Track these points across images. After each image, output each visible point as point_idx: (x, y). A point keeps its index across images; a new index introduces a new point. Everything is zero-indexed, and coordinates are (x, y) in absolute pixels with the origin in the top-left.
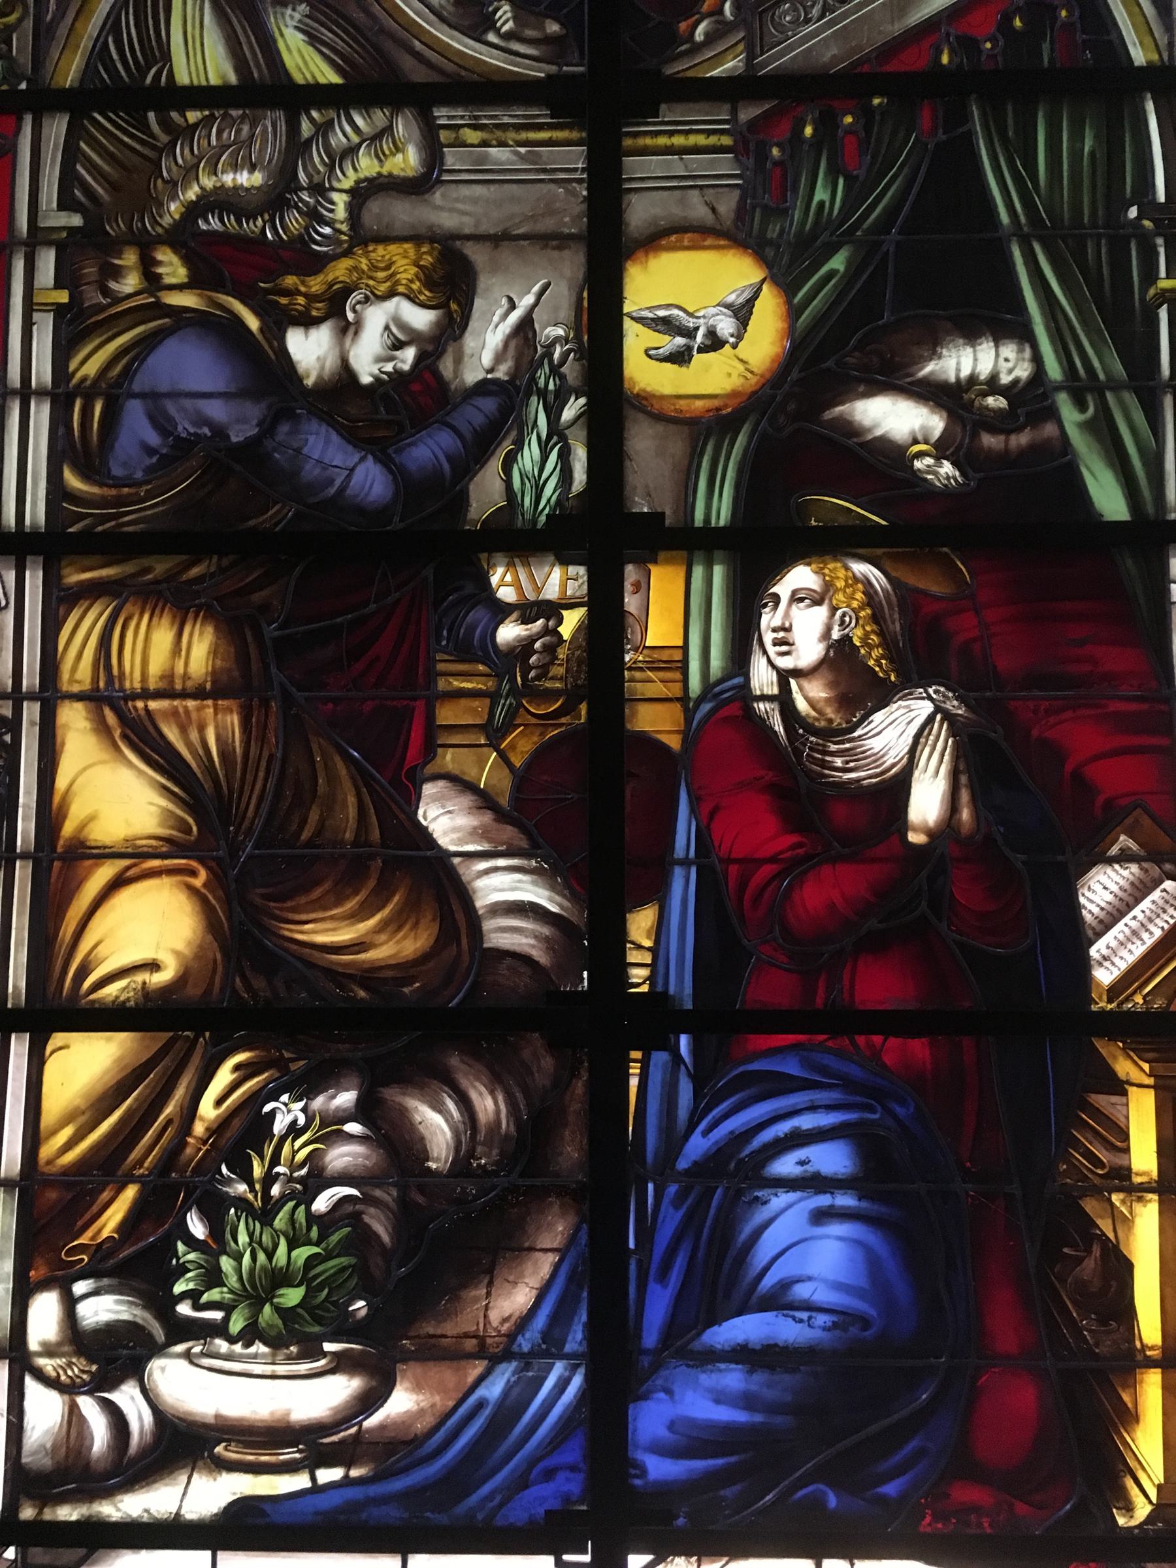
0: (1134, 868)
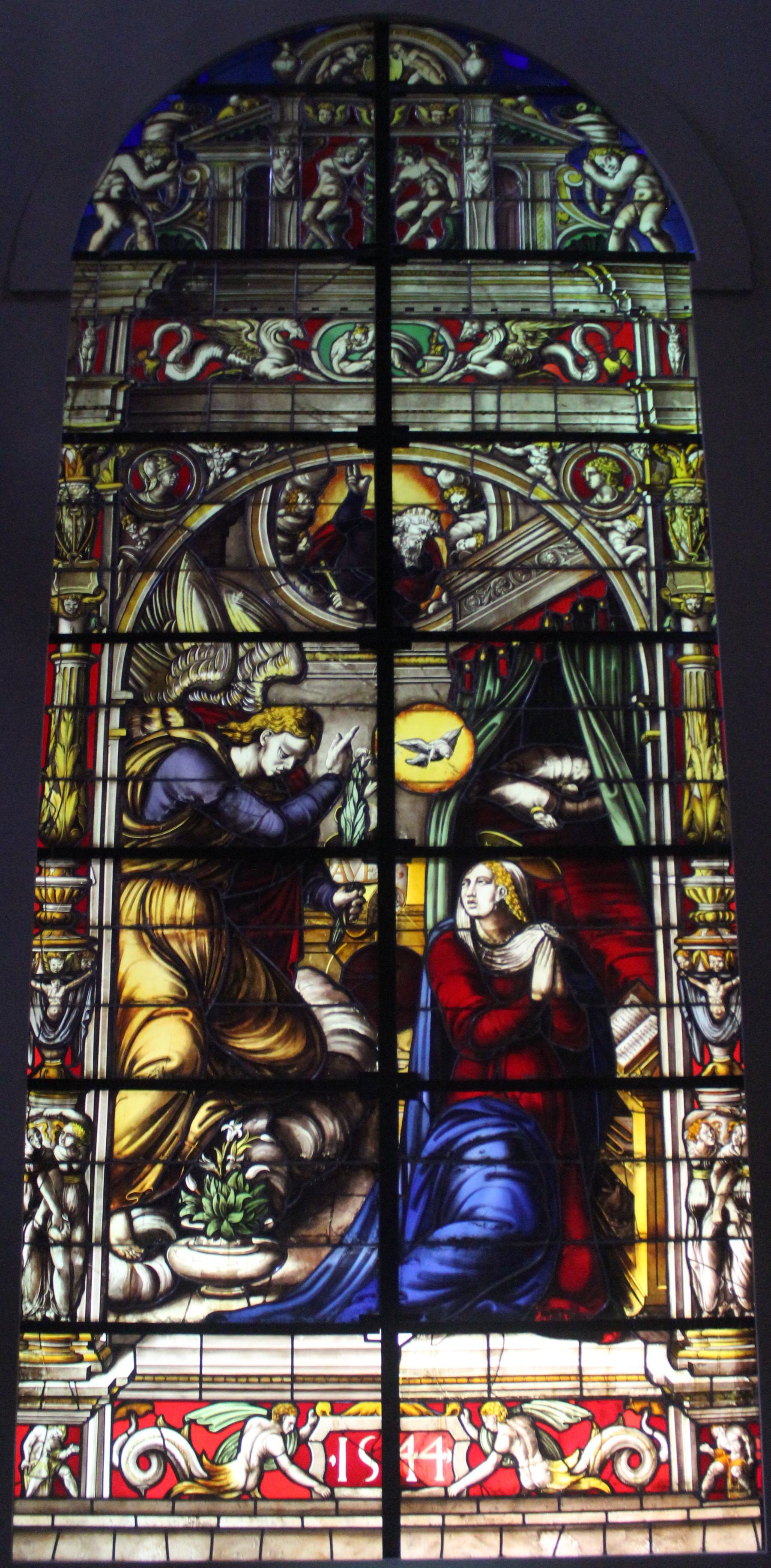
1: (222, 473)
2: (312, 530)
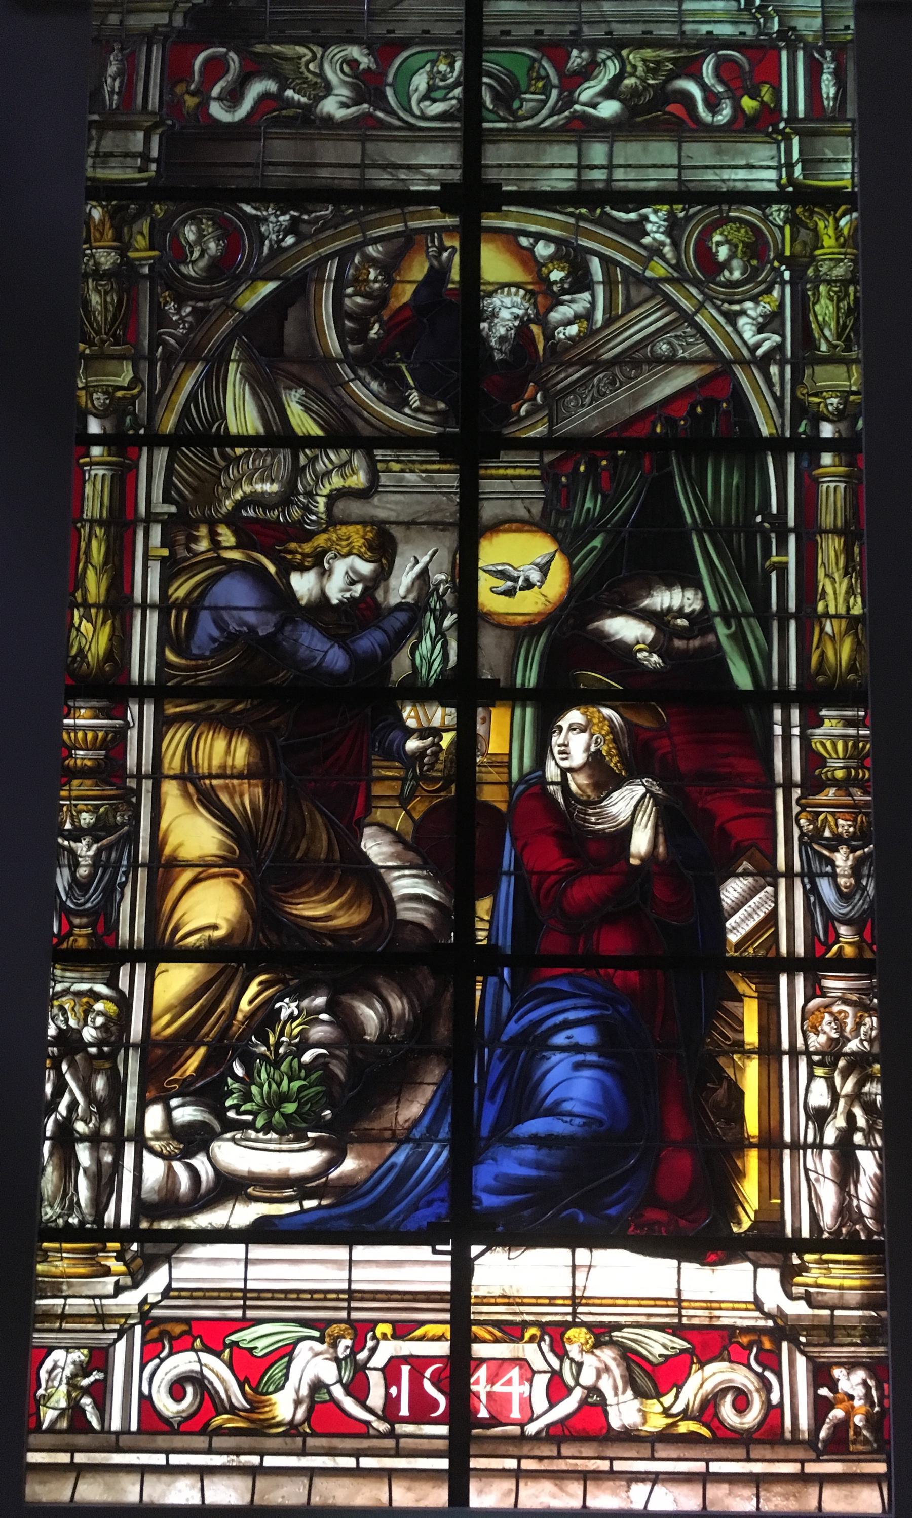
0: (751, 879)
1: (279, 241)
2: (386, 314)
